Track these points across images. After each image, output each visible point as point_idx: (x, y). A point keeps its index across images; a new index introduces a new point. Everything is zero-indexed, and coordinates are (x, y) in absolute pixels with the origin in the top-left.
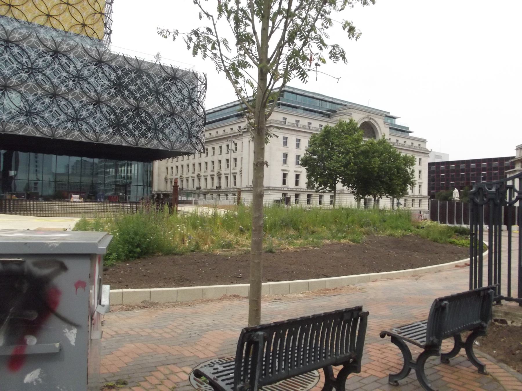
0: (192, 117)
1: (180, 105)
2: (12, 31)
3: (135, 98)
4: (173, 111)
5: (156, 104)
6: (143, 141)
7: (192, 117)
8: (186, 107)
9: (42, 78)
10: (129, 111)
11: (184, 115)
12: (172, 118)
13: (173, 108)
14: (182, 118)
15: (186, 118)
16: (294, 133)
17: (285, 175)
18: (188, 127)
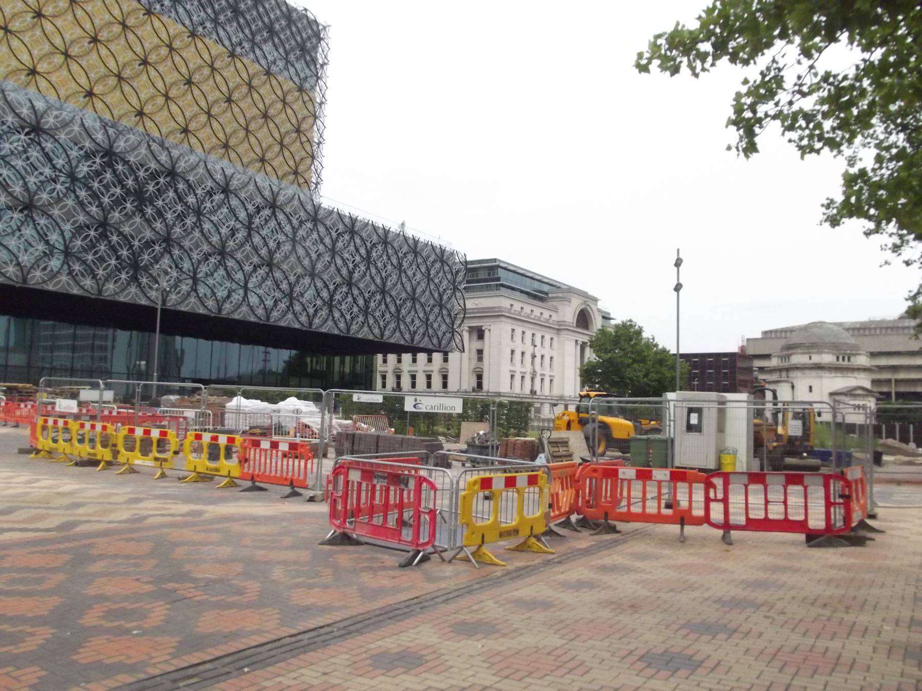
0: (74, 216)
1: (48, 189)
2: (45, 112)
3: (100, 205)
4: (31, 200)
5: (138, 219)
6: (111, 287)
7: (74, 216)
8: (61, 195)
9: (10, 173)
10: (154, 243)
11: (56, 212)
12: (27, 216)
13: (31, 195)
14: (50, 216)
15: (60, 217)
16: (520, 323)
17: (512, 376)
18: (64, 238)
